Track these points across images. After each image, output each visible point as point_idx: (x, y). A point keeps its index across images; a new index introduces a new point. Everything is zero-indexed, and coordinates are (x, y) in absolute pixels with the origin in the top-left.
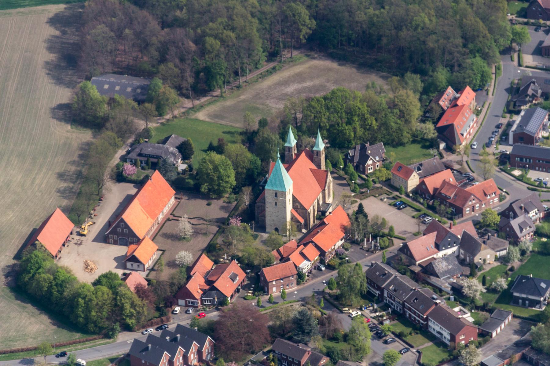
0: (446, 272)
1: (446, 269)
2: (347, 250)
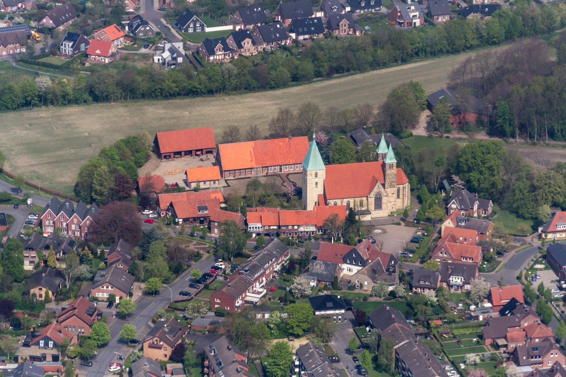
0: (317, 274)
1: (320, 271)
2: (316, 239)
